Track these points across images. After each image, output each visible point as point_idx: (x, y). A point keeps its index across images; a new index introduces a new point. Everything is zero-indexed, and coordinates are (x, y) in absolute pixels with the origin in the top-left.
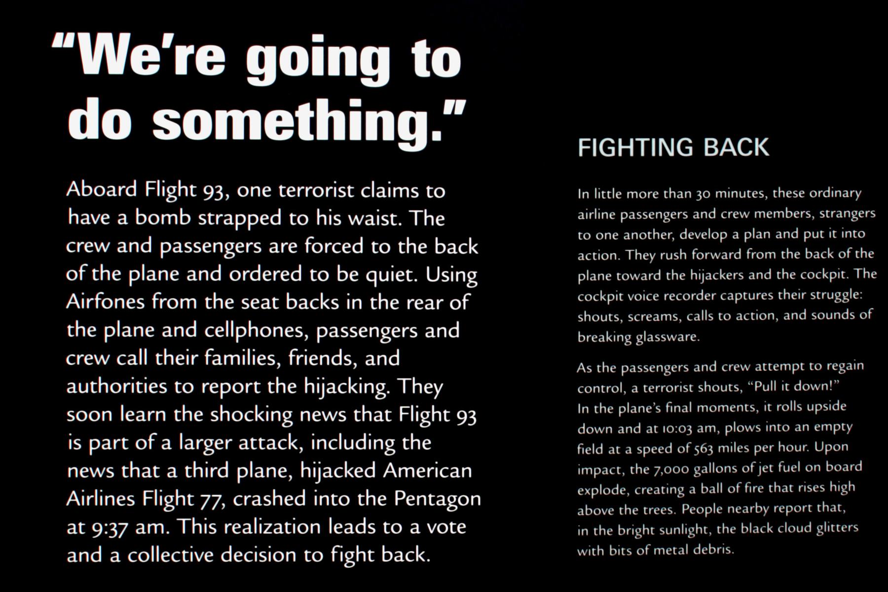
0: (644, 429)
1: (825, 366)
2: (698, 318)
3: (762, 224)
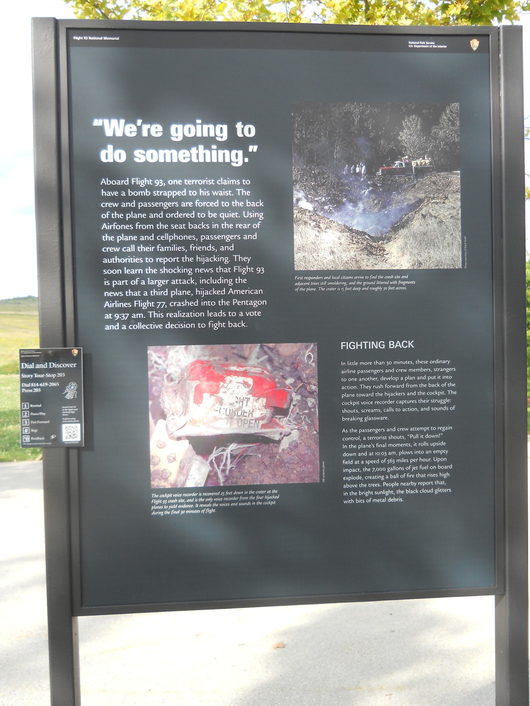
0: (368, 454)
1: (437, 428)
2: (388, 411)
3: (412, 374)
